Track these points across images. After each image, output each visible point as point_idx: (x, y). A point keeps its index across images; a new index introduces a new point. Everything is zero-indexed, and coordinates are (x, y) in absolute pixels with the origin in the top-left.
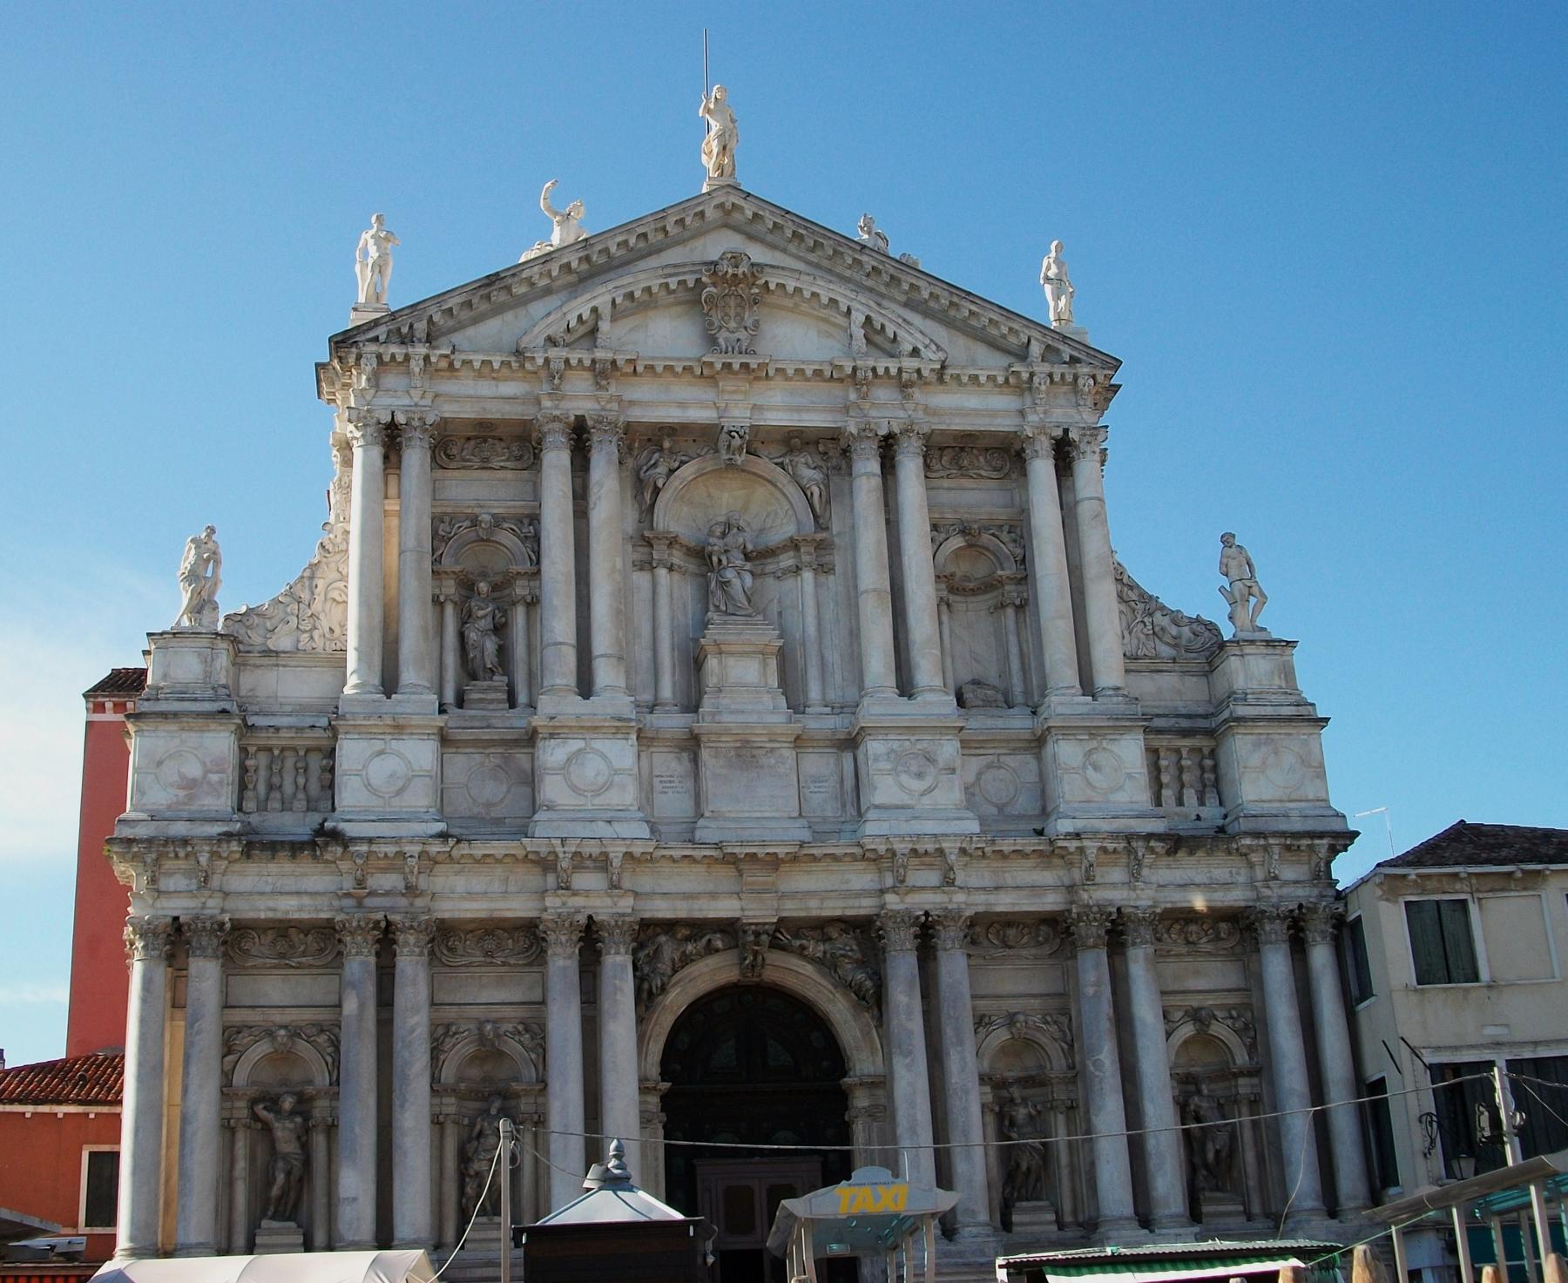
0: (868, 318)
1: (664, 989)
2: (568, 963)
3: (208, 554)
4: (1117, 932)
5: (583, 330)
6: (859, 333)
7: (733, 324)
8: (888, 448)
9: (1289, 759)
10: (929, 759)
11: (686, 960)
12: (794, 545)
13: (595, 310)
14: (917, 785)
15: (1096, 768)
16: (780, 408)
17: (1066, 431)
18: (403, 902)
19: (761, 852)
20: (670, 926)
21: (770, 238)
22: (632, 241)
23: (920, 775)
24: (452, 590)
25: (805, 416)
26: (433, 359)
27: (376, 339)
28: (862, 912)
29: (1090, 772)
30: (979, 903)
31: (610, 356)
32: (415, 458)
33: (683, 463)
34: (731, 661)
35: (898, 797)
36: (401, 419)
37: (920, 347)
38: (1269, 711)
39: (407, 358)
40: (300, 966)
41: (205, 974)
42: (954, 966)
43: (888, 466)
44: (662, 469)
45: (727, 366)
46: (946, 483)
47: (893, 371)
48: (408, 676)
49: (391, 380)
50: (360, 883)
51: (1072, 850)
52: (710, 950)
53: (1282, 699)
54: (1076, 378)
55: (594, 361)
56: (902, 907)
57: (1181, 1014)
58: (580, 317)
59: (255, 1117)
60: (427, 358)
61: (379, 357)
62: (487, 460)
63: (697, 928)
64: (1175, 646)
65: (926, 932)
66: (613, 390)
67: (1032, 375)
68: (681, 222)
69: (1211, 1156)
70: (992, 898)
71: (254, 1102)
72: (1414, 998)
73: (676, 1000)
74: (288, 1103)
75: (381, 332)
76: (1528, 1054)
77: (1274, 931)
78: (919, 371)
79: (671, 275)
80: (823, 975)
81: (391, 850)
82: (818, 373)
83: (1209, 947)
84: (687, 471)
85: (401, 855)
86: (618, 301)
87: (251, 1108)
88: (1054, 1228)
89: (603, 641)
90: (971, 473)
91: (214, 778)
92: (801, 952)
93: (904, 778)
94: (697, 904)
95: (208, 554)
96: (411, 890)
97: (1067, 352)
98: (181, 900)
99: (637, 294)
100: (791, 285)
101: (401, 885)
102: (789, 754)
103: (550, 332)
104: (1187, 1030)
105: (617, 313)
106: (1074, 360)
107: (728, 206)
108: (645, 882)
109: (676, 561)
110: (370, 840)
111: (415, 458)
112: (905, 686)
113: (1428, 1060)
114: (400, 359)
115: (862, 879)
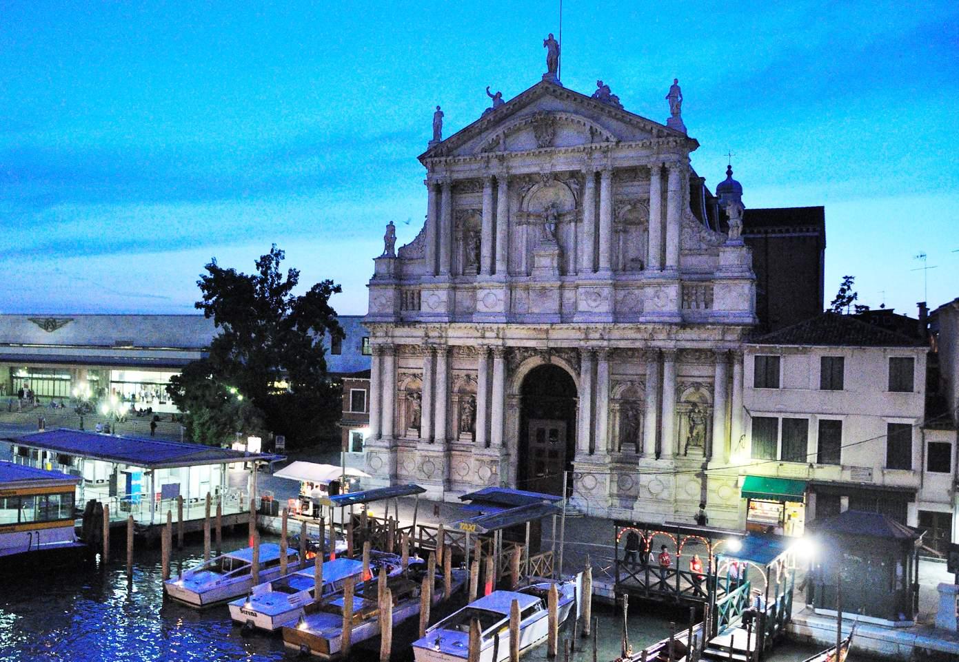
0: (591, 127)
1: (518, 367)
3: (391, 228)
4: (660, 356)
8: (598, 176)
11: (525, 358)
12: (569, 213)
14: (594, 304)
17: (664, 164)
20: (519, 348)
22: (511, 107)
23: (595, 300)
29: (656, 299)
30: (614, 344)
32: (445, 197)
34: (541, 259)
36: (440, 182)
38: (730, 274)
39: (440, 162)
41: (389, 361)
42: (603, 367)
48: (442, 269)
53: (737, 270)
60: (446, 161)
63: (526, 349)
66: (505, 164)
72: (751, 392)
73: (524, 370)
74: (415, 395)
75: (432, 153)
76: (792, 416)
89: (498, 256)
92: (558, 356)
93: (589, 301)
95: (391, 228)
97: (666, 131)
100: (564, 117)
111: (445, 197)
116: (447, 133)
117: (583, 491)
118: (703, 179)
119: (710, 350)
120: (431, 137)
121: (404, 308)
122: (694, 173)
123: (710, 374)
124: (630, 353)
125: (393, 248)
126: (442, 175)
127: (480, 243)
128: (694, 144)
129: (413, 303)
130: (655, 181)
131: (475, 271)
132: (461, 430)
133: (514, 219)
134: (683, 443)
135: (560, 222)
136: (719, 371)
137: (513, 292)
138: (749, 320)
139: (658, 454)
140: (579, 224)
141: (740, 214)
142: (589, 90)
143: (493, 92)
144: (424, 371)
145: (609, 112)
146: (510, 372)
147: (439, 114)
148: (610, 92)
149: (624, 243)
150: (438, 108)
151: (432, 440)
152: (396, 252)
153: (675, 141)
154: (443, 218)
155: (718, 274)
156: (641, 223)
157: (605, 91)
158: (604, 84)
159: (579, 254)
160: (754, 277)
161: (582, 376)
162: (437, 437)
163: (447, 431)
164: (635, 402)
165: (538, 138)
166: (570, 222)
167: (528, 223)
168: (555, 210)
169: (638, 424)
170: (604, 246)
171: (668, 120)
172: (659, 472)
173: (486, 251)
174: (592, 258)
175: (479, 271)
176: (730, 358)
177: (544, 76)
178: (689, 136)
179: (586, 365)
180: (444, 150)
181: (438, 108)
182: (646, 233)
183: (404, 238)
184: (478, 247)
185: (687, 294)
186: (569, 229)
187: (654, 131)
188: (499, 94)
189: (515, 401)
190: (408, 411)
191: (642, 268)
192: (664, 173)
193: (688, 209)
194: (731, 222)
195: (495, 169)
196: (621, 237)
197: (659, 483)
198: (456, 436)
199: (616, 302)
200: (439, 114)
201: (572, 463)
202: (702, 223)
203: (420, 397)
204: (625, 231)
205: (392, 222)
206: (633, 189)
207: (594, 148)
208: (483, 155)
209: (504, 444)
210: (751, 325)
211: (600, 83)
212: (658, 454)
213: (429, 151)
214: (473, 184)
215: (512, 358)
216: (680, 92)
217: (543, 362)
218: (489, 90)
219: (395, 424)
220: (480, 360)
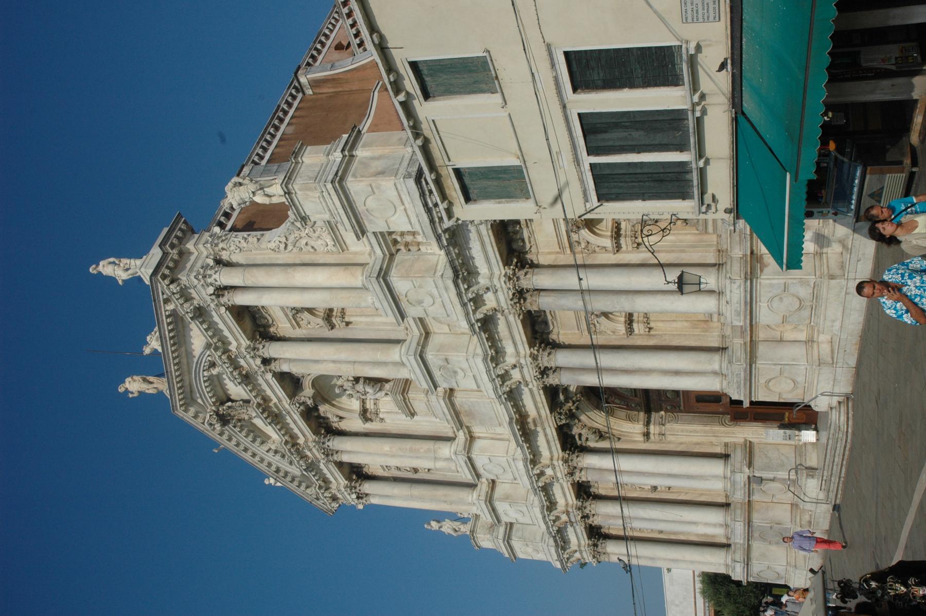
109: (372, 407)
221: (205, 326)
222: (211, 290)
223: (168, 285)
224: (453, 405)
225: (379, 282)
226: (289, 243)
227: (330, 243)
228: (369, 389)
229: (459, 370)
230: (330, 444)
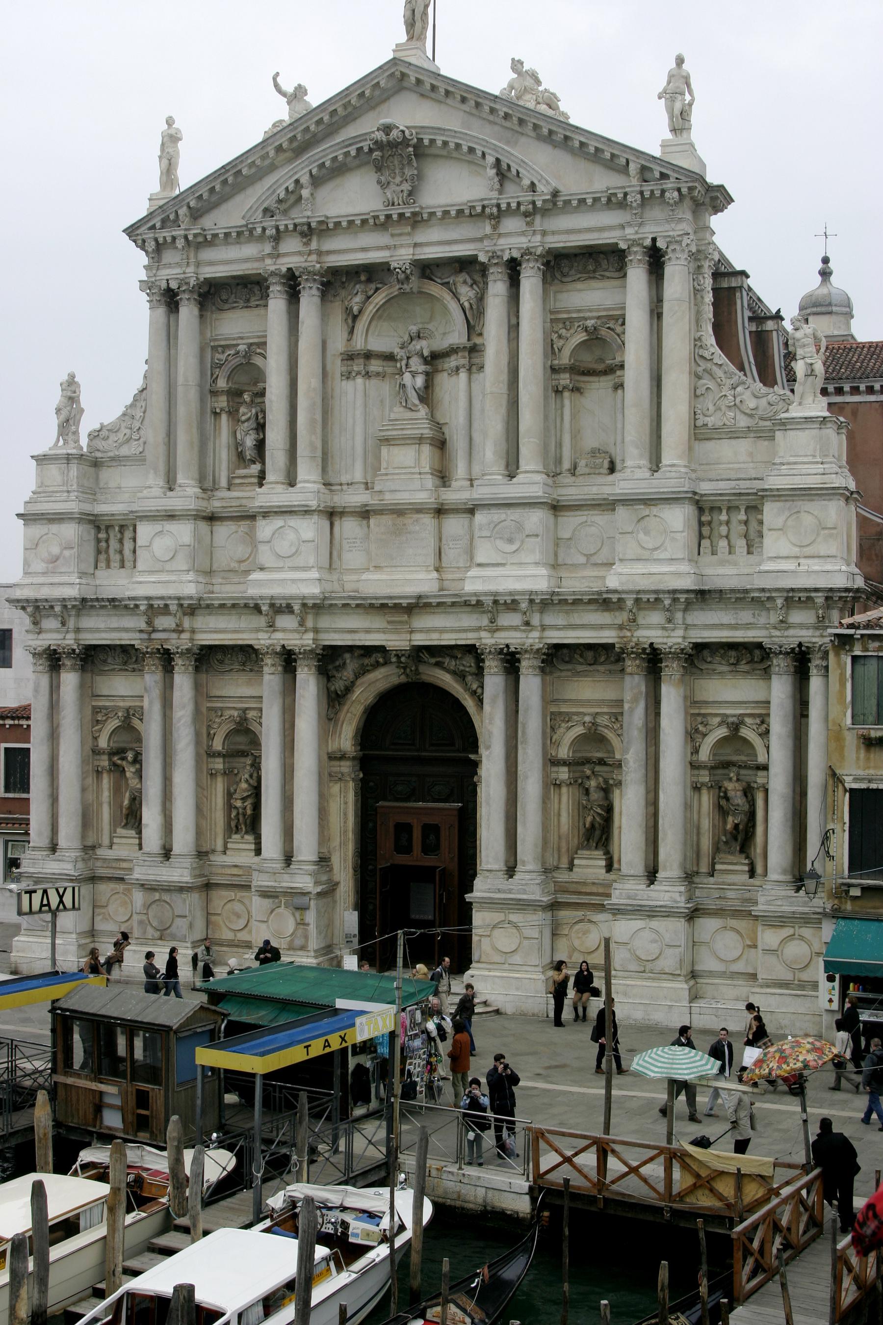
0: (498, 160)
1: (348, 689)
2: (272, 677)
4: (653, 660)
5: (292, 198)
6: (492, 172)
7: (398, 179)
8: (513, 268)
9: (807, 520)
10: (520, 527)
11: (362, 671)
13: (297, 181)
15: (647, 532)
16: (437, 243)
17: (654, 240)
18: (174, 635)
19: (390, 602)
20: (350, 649)
21: (433, 95)
22: (326, 118)
23: (510, 541)
24: (225, 404)
25: (455, 247)
26: (190, 238)
27: (153, 227)
28: (469, 642)
29: (641, 536)
31: (305, 220)
32: (188, 312)
33: (377, 289)
34: (395, 450)
35: (495, 558)
36: (174, 285)
37: (536, 182)
39: (174, 238)
40: (134, 670)
42: (531, 684)
43: (514, 281)
44: (358, 299)
45: (388, 217)
46: (579, 285)
47: (514, 205)
48: (181, 479)
49: (169, 256)
50: (149, 623)
51: (615, 600)
52: (377, 665)
54: (663, 192)
55: (295, 225)
56: (493, 641)
57: (718, 719)
58: (287, 189)
59: (115, 764)
60: (186, 237)
61: (156, 240)
62: (248, 301)
63: (368, 651)
64: (751, 416)
65: (511, 661)
66: (314, 245)
67: (626, 194)
68: (362, 95)
69: (729, 826)
70: (561, 634)
71: (112, 753)
74: (130, 756)
77: (780, 664)
78: (534, 203)
79: (350, 145)
80: (457, 681)
81: (161, 603)
82: (460, 212)
83: (746, 668)
84: (379, 299)
85: (166, 606)
86: (314, 171)
87: (110, 760)
88: (604, 871)
90: (597, 275)
91: (67, 553)
92: (438, 665)
93: (500, 544)
94: (356, 636)
96: (179, 630)
97: (657, 170)
98: (53, 636)
99: (328, 164)
101: (173, 626)
102: (428, 521)
103: (265, 205)
104: (723, 732)
105: (316, 181)
106: (664, 176)
107: (398, 74)
108: (325, 622)
110: (148, 598)
111: (188, 312)
112: (512, 469)
113: (848, 786)
114: (169, 240)
115: (468, 620)
116: (189, 175)
117: (497, 958)
118: (744, 274)
119: (759, 646)
120: (155, 187)
121: (102, 565)
122: (723, 260)
123: (763, 699)
124: (590, 654)
125: (76, 433)
126: (177, 270)
127: (264, 418)
128: (717, 199)
129: (121, 552)
130: (637, 276)
131: (255, 480)
132: (233, 828)
133: (337, 367)
134: (706, 843)
135: (436, 371)
136: (780, 689)
137: (337, 524)
138: (840, 582)
139: (652, 875)
140: (474, 376)
141: (818, 351)
142: (494, 81)
143: (289, 89)
144: (146, 704)
145: (536, 127)
146: (334, 700)
147: (171, 139)
148: (538, 82)
149: (573, 416)
150: (170, 122)
151: (167, 853)
152: (84, 441)
153: (679, 190)
154: (181, 370)
155: (774, 482)
156: (610, 371)
157: (529, 82)
158: (526, 67)
159: (476, 436)
160: (852, 486)
161: (487, 707)
162: (177, 849)
163: (199, 833)
164: (602, 762)
165: (384, 185)
166: (457, 369)
167: (367, 375)
168: (424, 343)
169: (609, 809)
170: (529, 419)
171: (664, 145)
172: (651, 913)
173: (276, 437)
174: (504, 446)
175: (261, 477)
176: (801, 660)
177: (399, 48)
178: (709, 179)
179: (494, 682)
180: (180, 212)
181: (170, 122)
182: (620, 391)
183: (102, 408)
184: (261, 427)
185: (710, 523)
186: (453, 387)
187: (632, 167)
188: (300, 92)
189: (346, 767)
190: (117, 791)
191: (612, 469)
192: (656, 260)
193: (710, 340)
194: (799, 367)
195: (293, 255)
196: (567, 402)
197: (654, 936)
198: (219, 846)
199: (557, 542)
200: (171, 139)
201: (468, 897)
202: (741, 368)
203: (137, 760)
204: (577, 390)
205: (72, 376)
206: (588, 297)
207: (504, 206)
208: (269, 223)
209: (323, 861)
210: (847, 590)
211: (517, 65)
212: (652, 875)
213: (150, 215)
214: (248, 288)
215: (338, 669)
216: (688, 85)
217: (403, 679)
218: (279, 79)
219: (87, 820)
220: (267, 677)
221: (589, 201)
222: (661, 244)
223: (679, 190)
224: (419, 511)
225: (687, 492)
226: (709, 365)
227: (711, 421)
228: (420, 381)
229: (514, 547)
230: (315, 292)
